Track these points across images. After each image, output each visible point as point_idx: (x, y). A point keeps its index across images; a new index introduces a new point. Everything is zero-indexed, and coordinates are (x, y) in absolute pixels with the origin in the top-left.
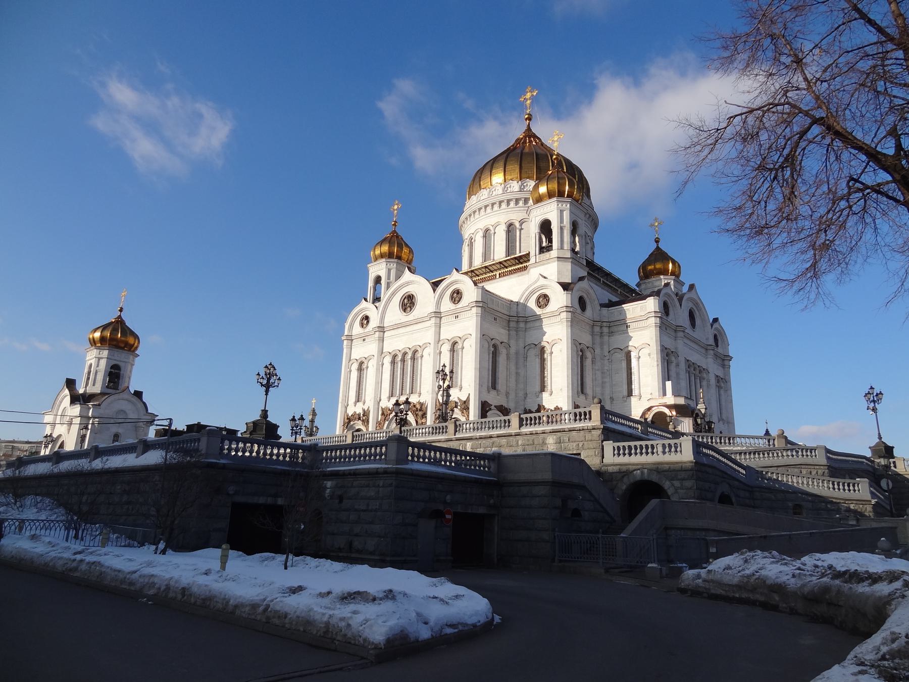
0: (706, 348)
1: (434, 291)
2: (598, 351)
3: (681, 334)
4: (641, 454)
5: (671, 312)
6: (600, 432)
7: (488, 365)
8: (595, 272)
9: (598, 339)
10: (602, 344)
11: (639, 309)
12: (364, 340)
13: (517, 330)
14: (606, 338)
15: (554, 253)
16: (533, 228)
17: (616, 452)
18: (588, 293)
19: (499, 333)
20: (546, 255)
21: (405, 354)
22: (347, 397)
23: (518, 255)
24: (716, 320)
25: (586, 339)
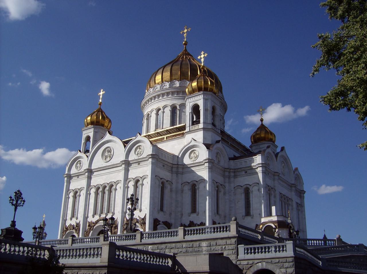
1: (125, 146)
3: (276, 177)
4: (262, 252)
6: (236, 239)
7: (159, 195)
8: (226, 138)
9: (227, 180)
10: (230, 183)
12: (78, 177)
13: (177, 173)
14: (232, 179)
15: (201, 126)
16: (188, 110)
17: (246, 251)
19: (166, 175)
20: (196, 127)
21: (105, 187)
22: (65, 214)
23: (178, 126)
24: (296, 169)
25: (220, 179)
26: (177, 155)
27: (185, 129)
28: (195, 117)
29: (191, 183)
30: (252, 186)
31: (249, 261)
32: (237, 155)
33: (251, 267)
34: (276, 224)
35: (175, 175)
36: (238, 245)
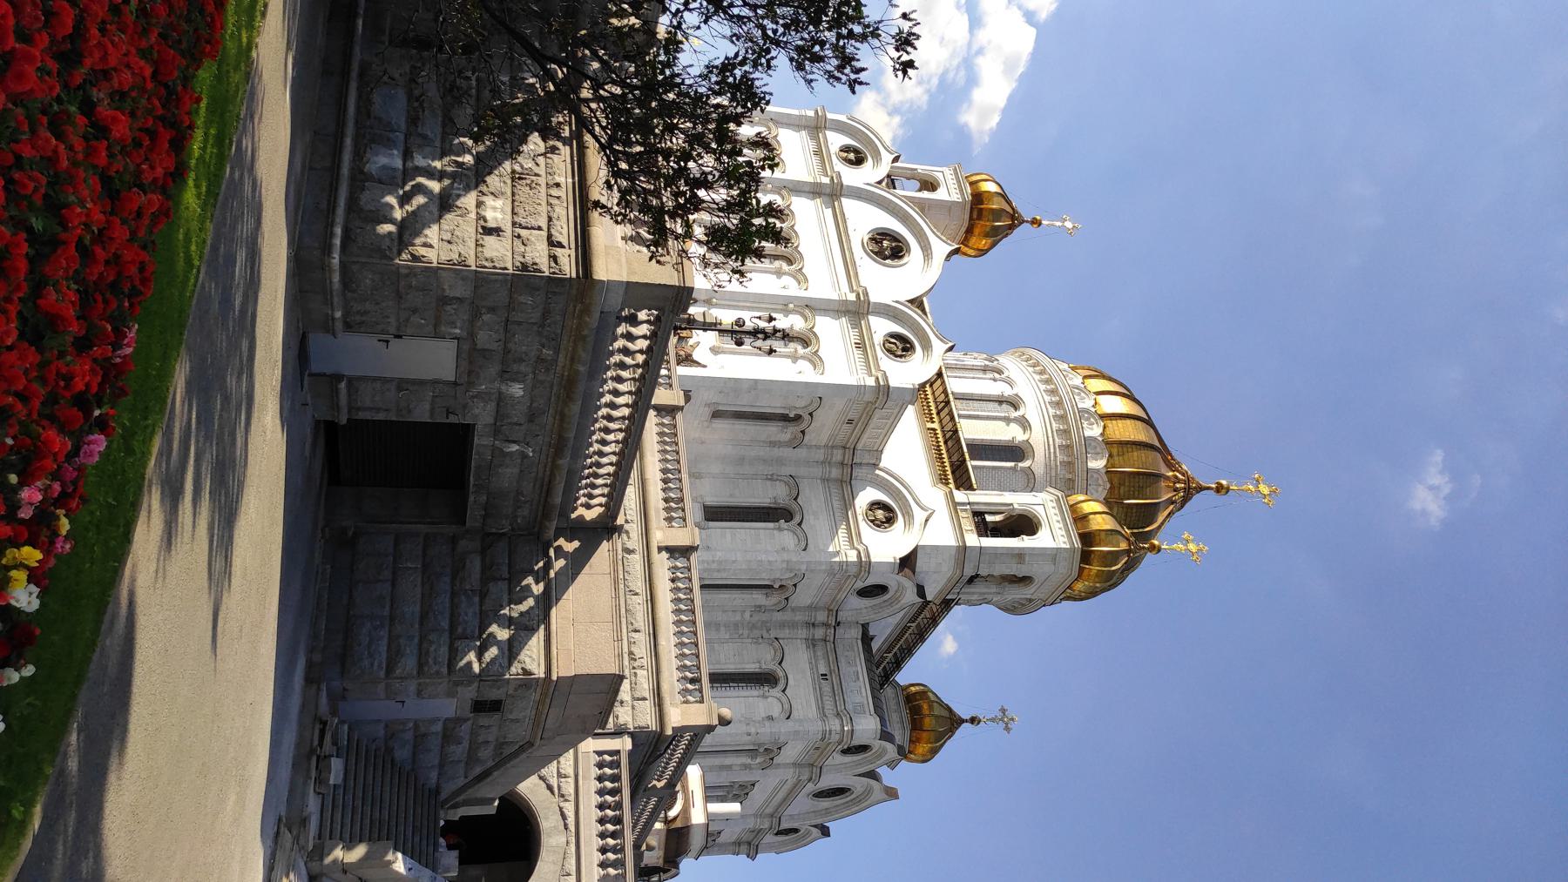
0: (775, 816)
1: (911, 301)
2: (778, 616)
5: (848, 759)
11: (858, 699)
14: (802, 633)
15: (973, 540)
18: (891, 603)
20: (968, 524)
23: (970, 464)
24: (825, 832)
26: (882, 465)
27: (958, 488)
28: (998, 518)
29: (794, 506)
30: (780, 695)
31: (571, 780)
32: (875, 646)
33: (550, 788)
34: (678, 824)
35: (820, 455)
36: (632, 735)
